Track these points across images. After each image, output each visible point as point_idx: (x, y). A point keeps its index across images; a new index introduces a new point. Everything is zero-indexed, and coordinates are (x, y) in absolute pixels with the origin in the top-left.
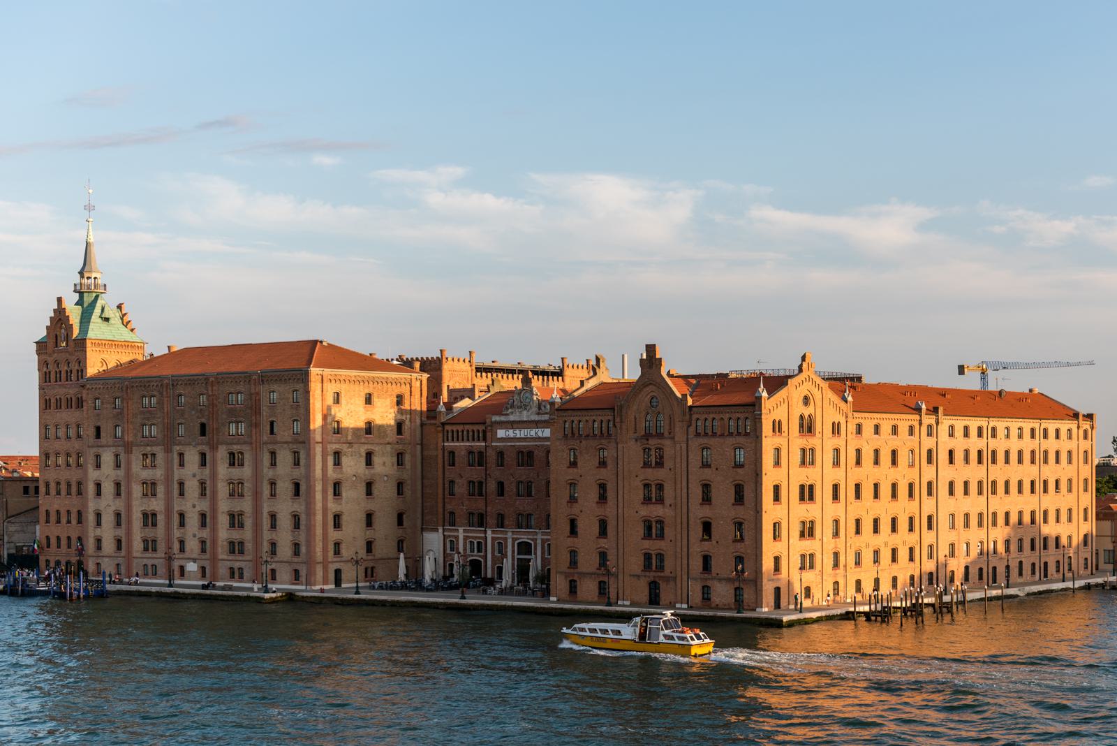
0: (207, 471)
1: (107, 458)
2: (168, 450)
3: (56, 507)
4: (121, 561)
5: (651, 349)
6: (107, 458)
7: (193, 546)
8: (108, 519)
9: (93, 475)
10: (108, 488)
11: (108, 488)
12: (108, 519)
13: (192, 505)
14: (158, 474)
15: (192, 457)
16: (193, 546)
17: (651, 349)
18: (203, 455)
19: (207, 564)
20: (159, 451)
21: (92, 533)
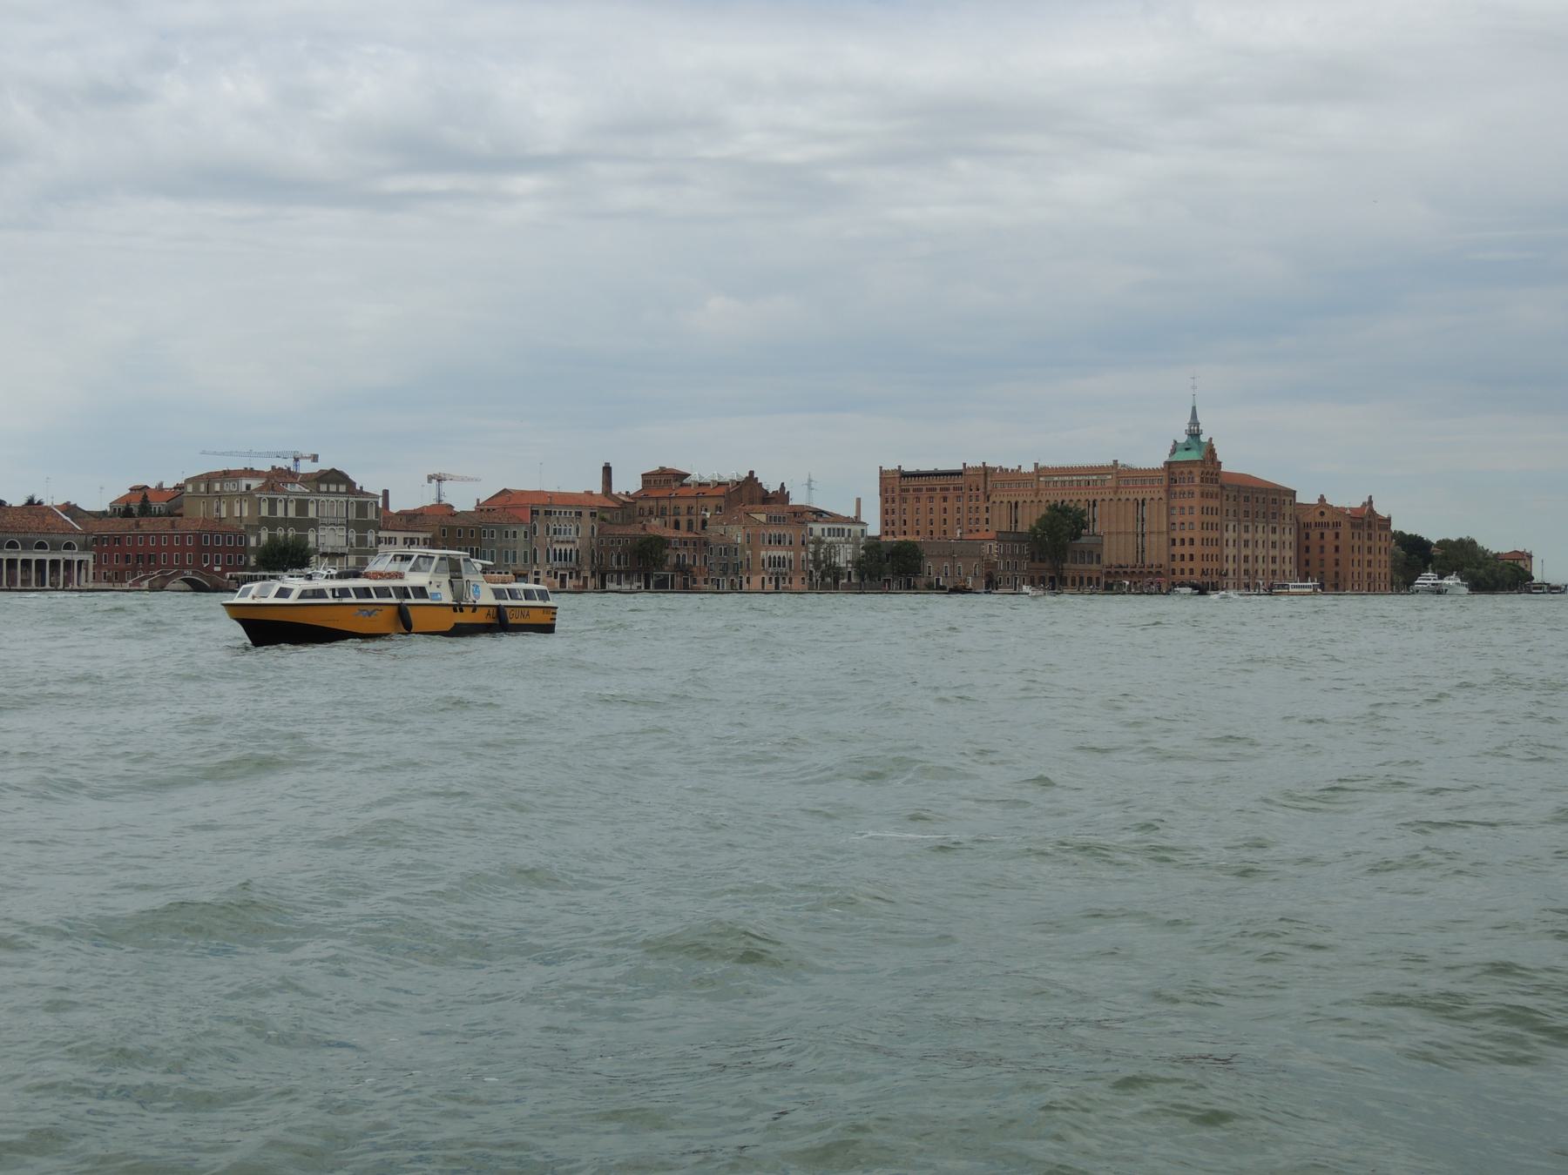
0: (1265, 535)
1: (1231, 527)
2: (1253, 525)
3: (1207, 552)
4: (1236, 581)
5: (1371, 497)
6: (1231, 527)
7: (1260, 572)
8: (1231, 559)
9: (1226, 535)
10: (1231, 543)
11: (1231, 543)
12: (1231, 559)
13: (1260, 552)
14: (1248, 536)
15: (1260, 529)
16: (1260, 572)
17: (1371, 497)
18: (1264, 527)
19: (1236, 581)
20: (1250, 524)
21: (1225, 567)
